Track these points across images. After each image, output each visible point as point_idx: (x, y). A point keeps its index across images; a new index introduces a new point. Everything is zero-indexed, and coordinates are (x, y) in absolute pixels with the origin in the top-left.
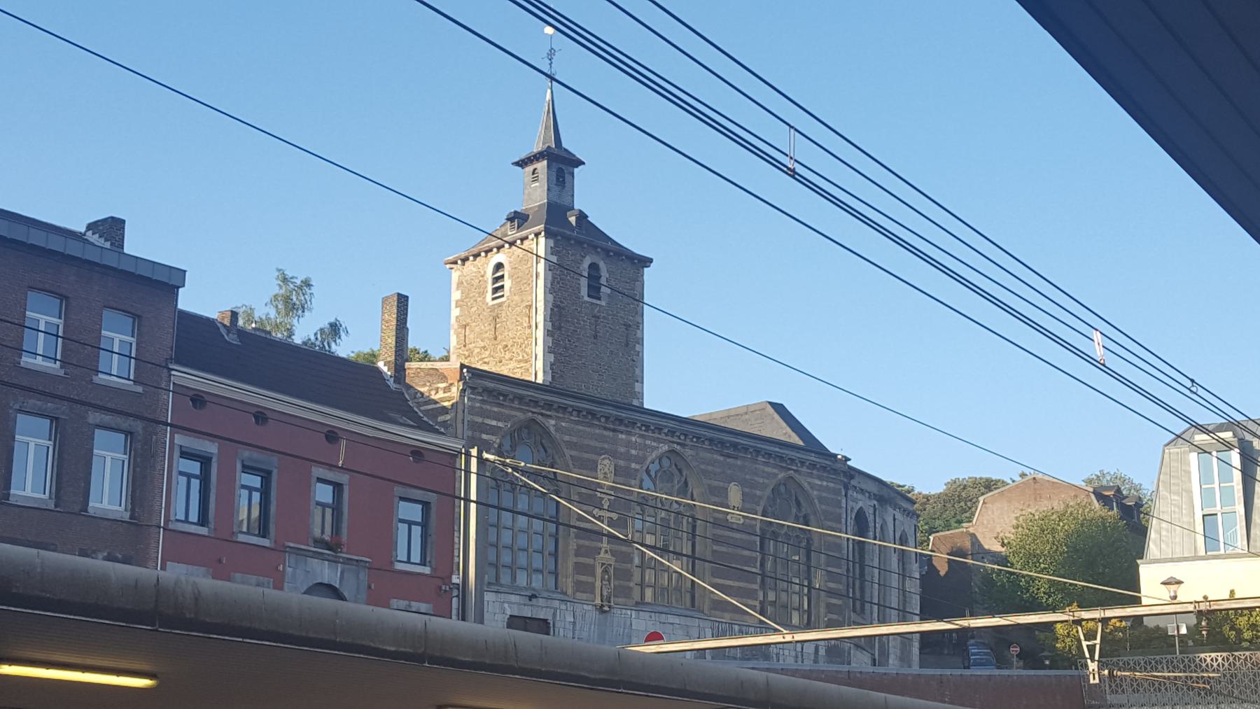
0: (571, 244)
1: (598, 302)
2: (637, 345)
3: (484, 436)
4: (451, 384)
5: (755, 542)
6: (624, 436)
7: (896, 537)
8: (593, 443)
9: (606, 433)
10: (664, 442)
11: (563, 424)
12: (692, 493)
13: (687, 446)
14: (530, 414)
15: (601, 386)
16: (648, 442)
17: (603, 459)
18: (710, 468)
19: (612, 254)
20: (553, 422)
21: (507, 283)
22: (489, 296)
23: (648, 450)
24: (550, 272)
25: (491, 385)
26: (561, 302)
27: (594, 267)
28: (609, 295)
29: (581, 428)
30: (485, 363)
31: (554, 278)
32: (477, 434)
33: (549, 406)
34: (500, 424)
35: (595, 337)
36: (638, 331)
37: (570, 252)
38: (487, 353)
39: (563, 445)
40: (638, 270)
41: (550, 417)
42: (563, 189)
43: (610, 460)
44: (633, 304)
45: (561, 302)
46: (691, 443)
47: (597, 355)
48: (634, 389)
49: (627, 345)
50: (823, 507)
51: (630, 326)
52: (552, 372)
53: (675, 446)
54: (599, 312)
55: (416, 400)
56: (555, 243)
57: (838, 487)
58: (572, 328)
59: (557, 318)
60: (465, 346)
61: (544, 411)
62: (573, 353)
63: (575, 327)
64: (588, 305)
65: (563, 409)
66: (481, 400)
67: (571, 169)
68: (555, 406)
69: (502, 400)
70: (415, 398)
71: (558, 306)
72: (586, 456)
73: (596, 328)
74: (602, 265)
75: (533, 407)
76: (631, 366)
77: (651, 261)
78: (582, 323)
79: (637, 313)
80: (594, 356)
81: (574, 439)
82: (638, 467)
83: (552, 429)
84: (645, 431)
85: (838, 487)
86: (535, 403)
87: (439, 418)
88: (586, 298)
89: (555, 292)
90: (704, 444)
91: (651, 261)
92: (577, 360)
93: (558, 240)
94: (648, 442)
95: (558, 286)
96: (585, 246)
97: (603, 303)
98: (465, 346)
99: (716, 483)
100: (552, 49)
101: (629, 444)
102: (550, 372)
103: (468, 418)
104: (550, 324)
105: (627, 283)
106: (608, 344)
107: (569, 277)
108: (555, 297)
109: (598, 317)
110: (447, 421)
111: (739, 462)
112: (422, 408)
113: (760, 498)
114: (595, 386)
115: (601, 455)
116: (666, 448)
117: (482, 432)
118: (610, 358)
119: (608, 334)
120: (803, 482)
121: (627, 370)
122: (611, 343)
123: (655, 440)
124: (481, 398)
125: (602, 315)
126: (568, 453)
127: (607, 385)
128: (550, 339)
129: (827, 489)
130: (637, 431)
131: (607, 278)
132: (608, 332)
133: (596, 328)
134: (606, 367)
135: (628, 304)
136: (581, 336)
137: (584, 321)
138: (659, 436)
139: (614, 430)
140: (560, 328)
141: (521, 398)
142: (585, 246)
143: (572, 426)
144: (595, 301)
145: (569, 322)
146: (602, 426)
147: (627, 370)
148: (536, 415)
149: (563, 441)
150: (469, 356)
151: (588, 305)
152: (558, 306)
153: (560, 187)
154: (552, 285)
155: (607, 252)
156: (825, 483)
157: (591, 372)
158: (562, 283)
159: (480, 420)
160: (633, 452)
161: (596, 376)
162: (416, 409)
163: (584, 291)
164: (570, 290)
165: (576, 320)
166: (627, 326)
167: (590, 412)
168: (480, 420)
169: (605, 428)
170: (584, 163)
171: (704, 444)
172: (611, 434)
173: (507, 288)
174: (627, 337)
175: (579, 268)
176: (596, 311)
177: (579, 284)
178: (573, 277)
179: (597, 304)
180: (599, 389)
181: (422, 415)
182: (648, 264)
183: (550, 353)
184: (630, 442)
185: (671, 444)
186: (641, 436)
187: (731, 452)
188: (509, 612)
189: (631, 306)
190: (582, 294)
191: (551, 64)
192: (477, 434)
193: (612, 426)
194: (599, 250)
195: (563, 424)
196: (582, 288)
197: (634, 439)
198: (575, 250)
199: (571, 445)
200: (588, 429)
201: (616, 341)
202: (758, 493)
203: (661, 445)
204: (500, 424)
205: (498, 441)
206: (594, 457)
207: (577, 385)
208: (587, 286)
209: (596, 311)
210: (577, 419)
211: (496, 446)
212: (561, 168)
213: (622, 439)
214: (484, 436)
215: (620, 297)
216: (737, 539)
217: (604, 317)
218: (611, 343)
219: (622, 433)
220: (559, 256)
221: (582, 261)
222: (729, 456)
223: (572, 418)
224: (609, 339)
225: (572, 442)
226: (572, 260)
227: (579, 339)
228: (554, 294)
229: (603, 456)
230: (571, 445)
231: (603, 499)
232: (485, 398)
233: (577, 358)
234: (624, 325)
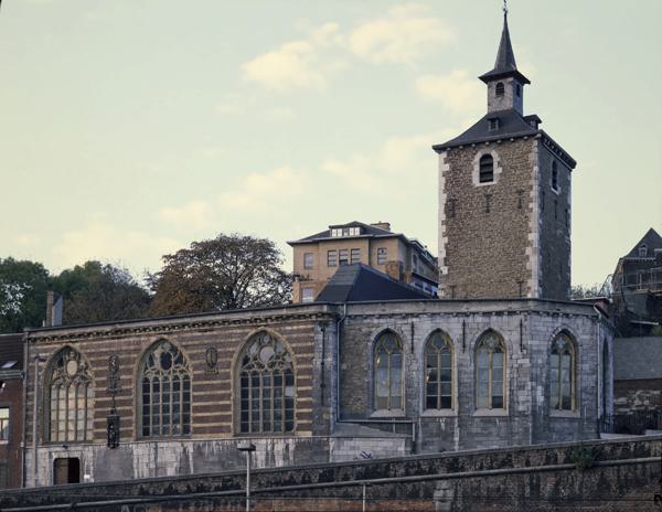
1: (490, 183)
5: (229, 384)
7: (469, 337)
8: (104, 350)
10: (154, 335)
18: (190, 343)
20: (78, 344)
31: (447, 181)
35: (488, 211)
49: (520, 207)
50: (294, 345)
57: (310, 326)
74: (494, 154)
82: (135, 356)
83: (78, 349)
85: (310, 326)
99: (195, 352)
111: (215, 333)
113: (234, 352)
128: (444, 227)
129: (298, 331)
140: (453, 216)
152: (450, 200)
156: (295, 328)
166: (520, 192)
169: (113, 338)
187: (206, 327)
188: (55, 456)
202: (231, 349)
222: (206, 331)
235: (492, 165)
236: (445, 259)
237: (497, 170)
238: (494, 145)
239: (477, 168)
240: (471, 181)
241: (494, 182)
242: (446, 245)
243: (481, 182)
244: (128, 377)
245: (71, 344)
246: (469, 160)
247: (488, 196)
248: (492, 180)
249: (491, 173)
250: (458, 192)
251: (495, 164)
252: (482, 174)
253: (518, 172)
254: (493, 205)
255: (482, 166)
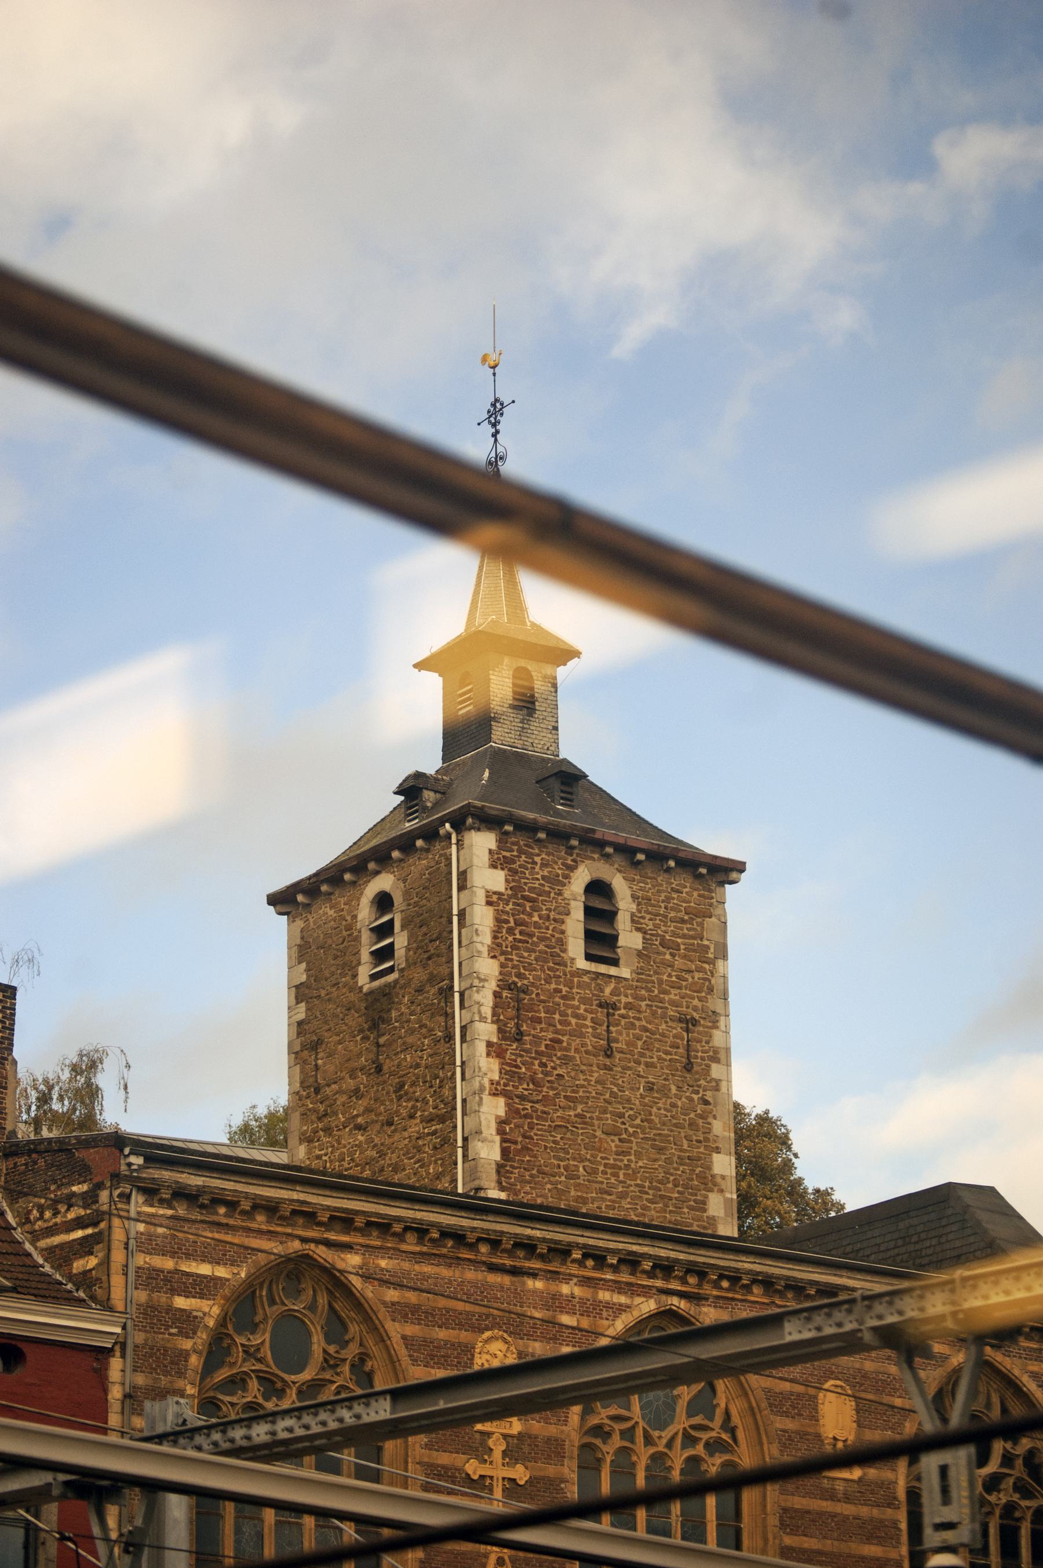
0: (539, 840)
1: (613, 971)
2: (714, 1066)
3: (181, 1302)
4: (99, 1186)
5: (895, 1524)
6: (539, 1284)
9: (495, 1278)
10: (646, 1292)
11: (383, 1263)
12: (727, 1414)
13: (707, 1299)
14: (297, 1245)
15: (627, 1167)
16: (604, 1296)
17: (487, 1341)
19: (641, 857)
20: (353, 1260)
21: (400, 940)
22: (364, 972)
23: (605, 1314)
24: (491, 909)
25: (194, 1180)
26: (519, 975)
27: (598, 888)
28: (639, 954)
29: (427, 1269)
30: (358, 1127)
31: (499, 921)
32: (162, 1298)
33: (345, 1221)
34: (221, 1272)
35: (608, 1053)
36: (715, 1032)
37: (537, 859)
38: (362, 1103)
39: (382, 1313)
40: (710, 891)
41: (348, 1247)
42: (530, 715)
43: (506, 1342)
44: (700, 970)
45: (519, 975)
46: (715, 1293)
47: (613, 1095)
48: (709, 1168)
49: (688, 1067)
51: (695, 1022)
52: (503, 1141)
53: (675, 1301)
54: (615, 992)
55: (27, 1227)
56: (500, 841)
58: (551, 1036)
59: (511, 1013)
60: (317, 1091)
61: (332, 1236)
62: (551, 1093)
63: (556, 1032)
64: (586, 979)
65: (383, 1227)
66: (172, 1217)
67: (548, 670)
68: (359, 1222)
69: (226, 1215)
70: (28, 1221)
71: (509, 987)
72: (442, 1334)
73: (608, 1031)
74: (619, 884)
75: (305, 1227)
76: (701, 1117)
77: (739, 867)
78: (573, 1021)
79: (711, 990)
80: (607, 1096)
81: (412, 1297)
84: (594, 1268)
86: (310, 1216)
87: (75, 1265)
88: (582, 964)
89: (503, 953)
90: (751, 1292)
91: (739, 867)
92: (563, 1108)
93: (506, 833)
94: (604, 1296)
95: (510, 939)
96: (575, 842)
97: (625, 972)
98: (317, 1091)
100: (497, 400)
101: (555, 1302)
102: (498, 1139)
103: (140, 1260)
104: (495, 1027)
105: (683, 921)
106: (641, 1069)
107: (536, 918)
108: (502, 966)
109: (614, 1006)
110: (91, 1270)
112: (43, 1244)
114: (613, 1167)
115: (482, 1331)
116: (648, 1306)
117: (174, 1292)
118: (646, 1100)
119: (640, 1043)
120: (1016, 1372)
121: (692, 1124)
122: (647, 1065)
123: (619, 1287)
124: (170, 1212)
125: (624, 999)
126: (395, 1330)
127: (640, 1164)
130: (574, 1270)
131: (633, 915)
132: (639, 1038)
133: (608, 1031)
134: (638, 1121)
135: (689, 971)
136: (572, 1054)
137: (577, 1016)
138: (632, 1279)
139: (514, 1272)
141: (271, 1208)
142: (575, 842)
143: (406, 1265)
144: (603, 969)
145: (539, 1021)
146: (484, 1263)
147: (692, 1124)
148: (312, 1246)
149: (384, 1303)
150: (325, 1115)
151: (586, 979)
152: (509, 987)
153: (525, 711)
154: (495, 937)
155: (627, 851)
157: (599, 1133)
158: (521, 933)
159: (169, 1264)
160: (566, 1319)
161: (613, 1143)
162: (28, 1246)
163: (576, 948)
164: (542, 947)
165: (557, 1016)
166: (689, 1023)
167: (446, 1233)
168: (169, 1264)
169: (493, 1268)
170: (576, 654)
171: (751, 1292)
172: (506, 1280)
173: (400, 952)
174: (688, 1048)
175: (560, 894)
176: (608, 991)
177: (563, 932)
178: (548, 918)
179: (610, 976)
180: (621, 1173)
181: (41, 1261)
182: (734, 875)
183: (494, 1095)
184: (556, 1296)
185: (663, 1297)
186: (586, 1282)
189: (697, 975)
190: (571, 954)
191: (495, 435)
192: (162, 1298)
193: (508, 1262)
194: (609, 850)
195: (383, 1263)
196: (571, 940)
197: (565, 1289)
198: (548, 854)
199: (403, 1312)
200: (445, 1272)
201: (659, 1058)
203: (638, 1300)
204: (221, 1272)
205: (216, 1311)
206: (464, 1336)
207: (566, 1168)
208: (582, 935)
209: (608, 991)
210: (417, 1249)
211: (211, 1323)
212: (526, 670)
213: (535, 1291)
214: (181, 1302)
215: (668, 957)
216: (847, 1517)
217: (628, 1006)
218: (647, 1065)
219: (534, 1275)
220: (510, 870)
221: (567, 877)
223: (404, 1247)
224: (642, 1055)
225: (407, 1305)
226: (543, 877)
227: (566, 1060)
228: (502, 958)
229: (488, 1334)
230: (403, 1312)
231: (489, 1434)
232: (181, 1212)
233: (563, 1102)
234: (680, 1021)
235: (610, 916)
236: (500, 1168)
237: (629, 939)
238: (619, 860)
239: (577, 913)
240: (562, 943)
241: (624, 972)
242: (501, 1123)
243: (589, 957)
244: (553, 1430)
245: (322, 1252)
246: (558, 882)
247: (609, 1007)
248: (615, 962)
249: (615, 938)
250: (529, 967)
251: (623, 922)
252: (590, 936)
253: (679, 962)
254: (622, 1039)
255: (589, 912)
